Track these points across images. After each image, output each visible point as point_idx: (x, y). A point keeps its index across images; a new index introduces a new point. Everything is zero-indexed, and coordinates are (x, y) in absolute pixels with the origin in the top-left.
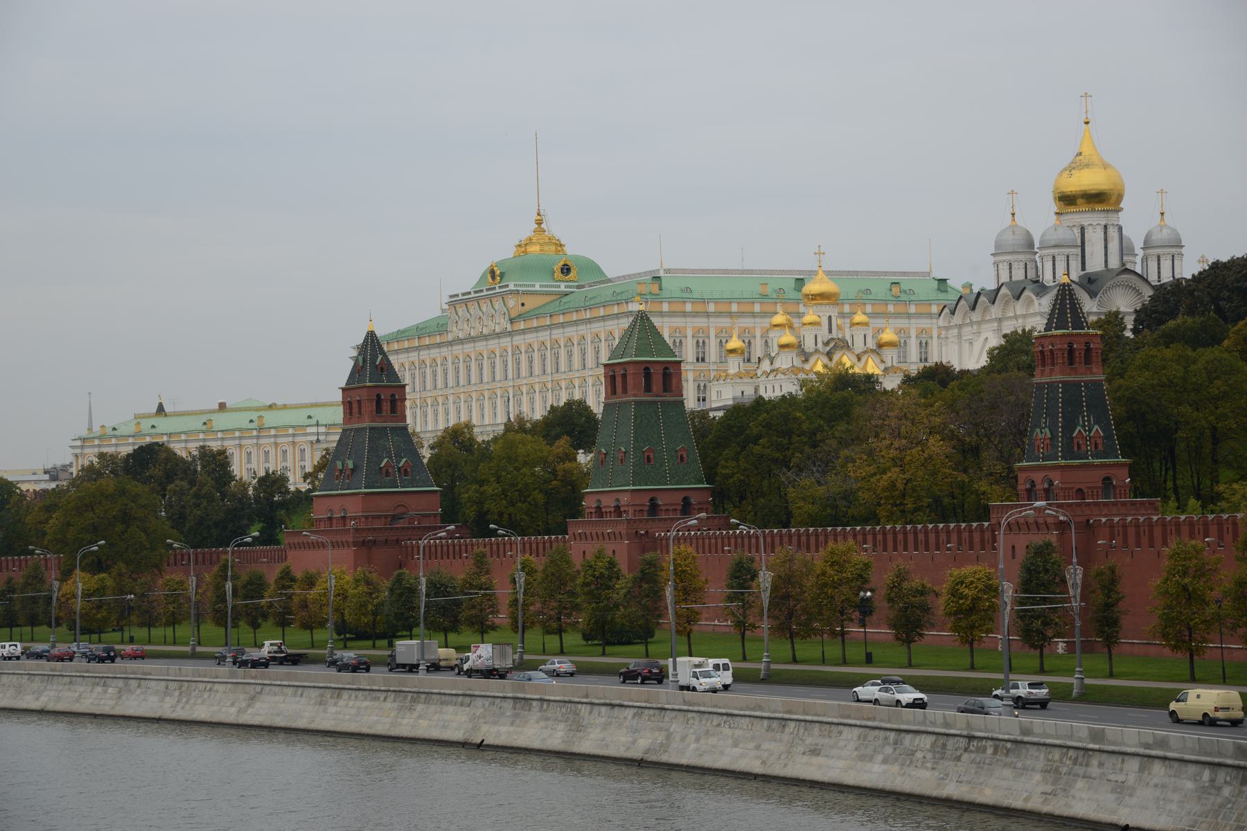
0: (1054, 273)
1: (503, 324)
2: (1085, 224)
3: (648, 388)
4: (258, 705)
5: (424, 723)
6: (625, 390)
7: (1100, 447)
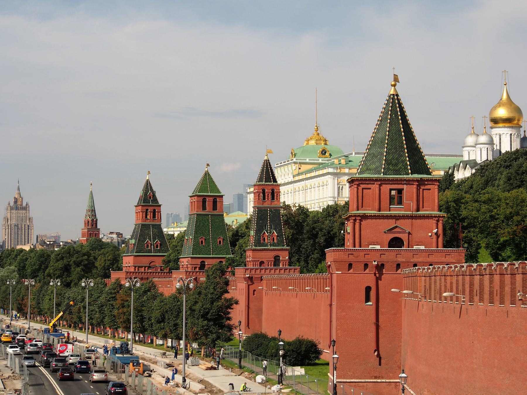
0: (481, 157)
2: (501, 133)
3: (204, 208)
6: (194, 210)
7: (275, 241)
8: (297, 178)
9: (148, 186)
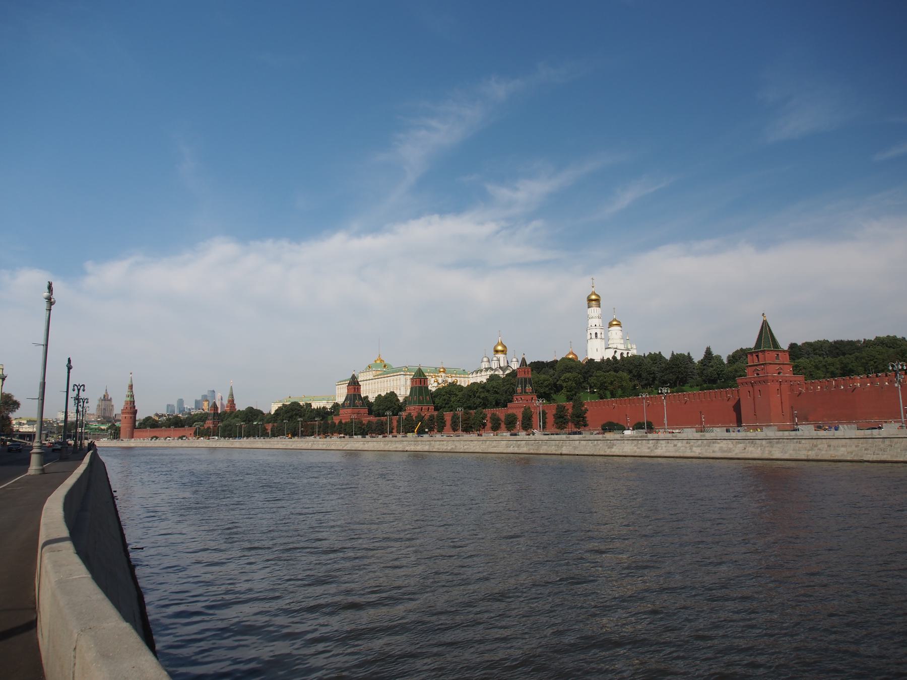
1: (371, 377)
3: (421, 384)
4: (347, 446)
5: (391, 447)
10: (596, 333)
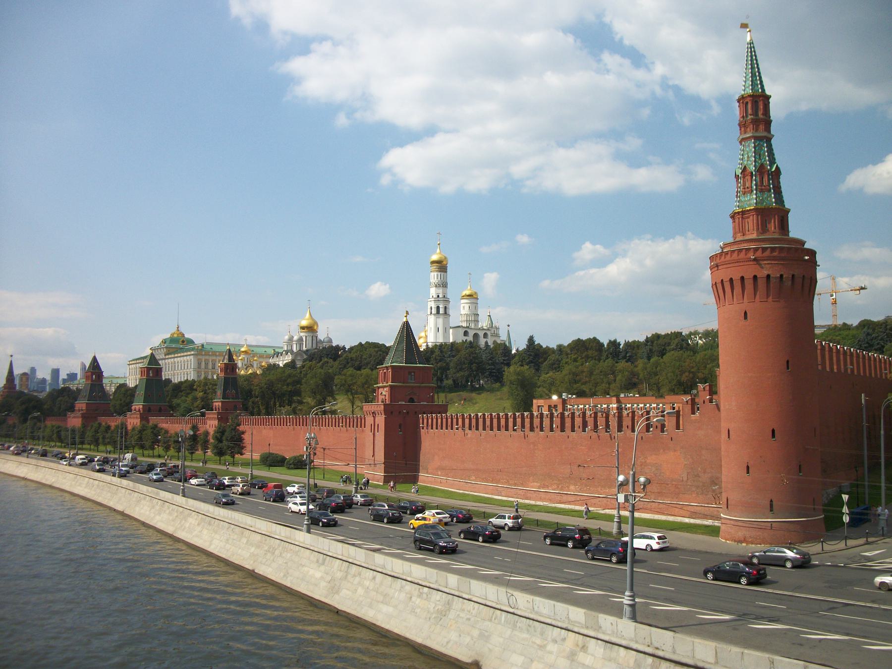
6: (144, 375)
8: (167, 357)
9: (95, 359)
10: (438, 308)
